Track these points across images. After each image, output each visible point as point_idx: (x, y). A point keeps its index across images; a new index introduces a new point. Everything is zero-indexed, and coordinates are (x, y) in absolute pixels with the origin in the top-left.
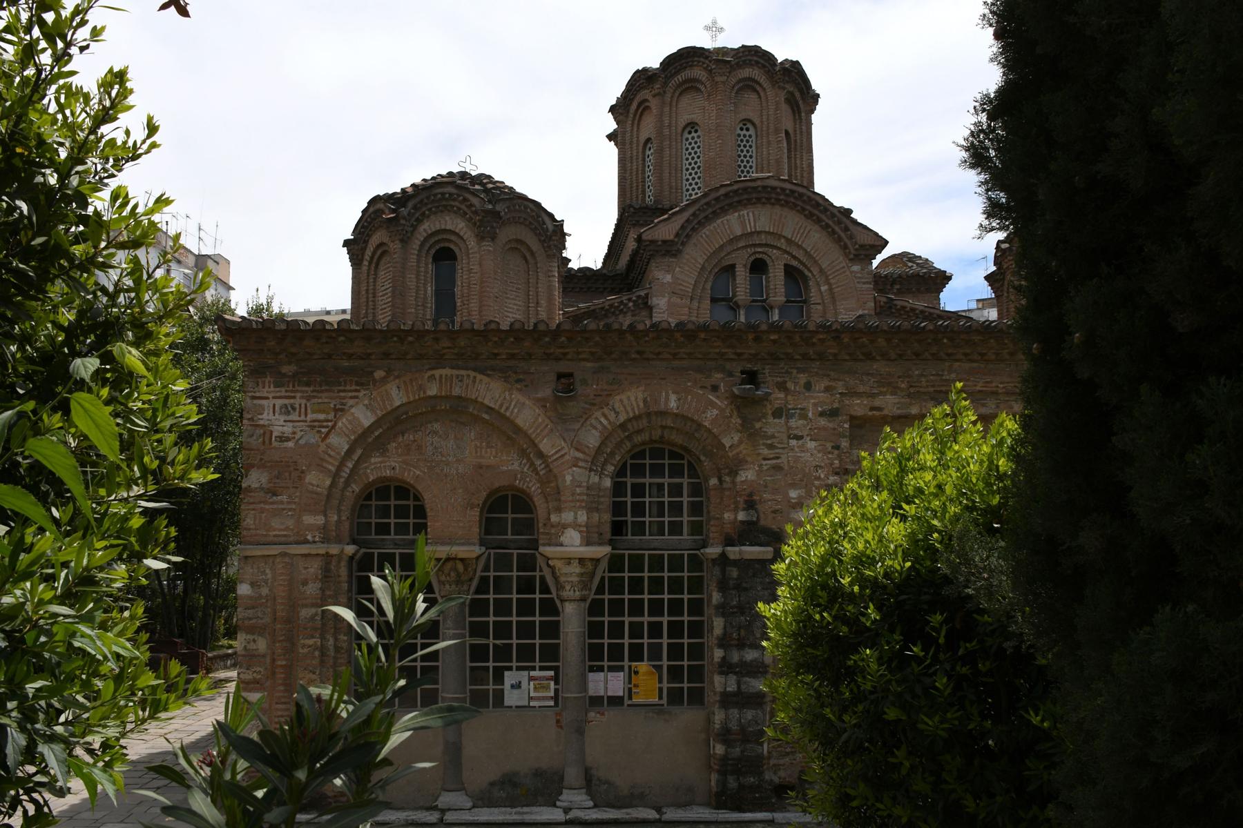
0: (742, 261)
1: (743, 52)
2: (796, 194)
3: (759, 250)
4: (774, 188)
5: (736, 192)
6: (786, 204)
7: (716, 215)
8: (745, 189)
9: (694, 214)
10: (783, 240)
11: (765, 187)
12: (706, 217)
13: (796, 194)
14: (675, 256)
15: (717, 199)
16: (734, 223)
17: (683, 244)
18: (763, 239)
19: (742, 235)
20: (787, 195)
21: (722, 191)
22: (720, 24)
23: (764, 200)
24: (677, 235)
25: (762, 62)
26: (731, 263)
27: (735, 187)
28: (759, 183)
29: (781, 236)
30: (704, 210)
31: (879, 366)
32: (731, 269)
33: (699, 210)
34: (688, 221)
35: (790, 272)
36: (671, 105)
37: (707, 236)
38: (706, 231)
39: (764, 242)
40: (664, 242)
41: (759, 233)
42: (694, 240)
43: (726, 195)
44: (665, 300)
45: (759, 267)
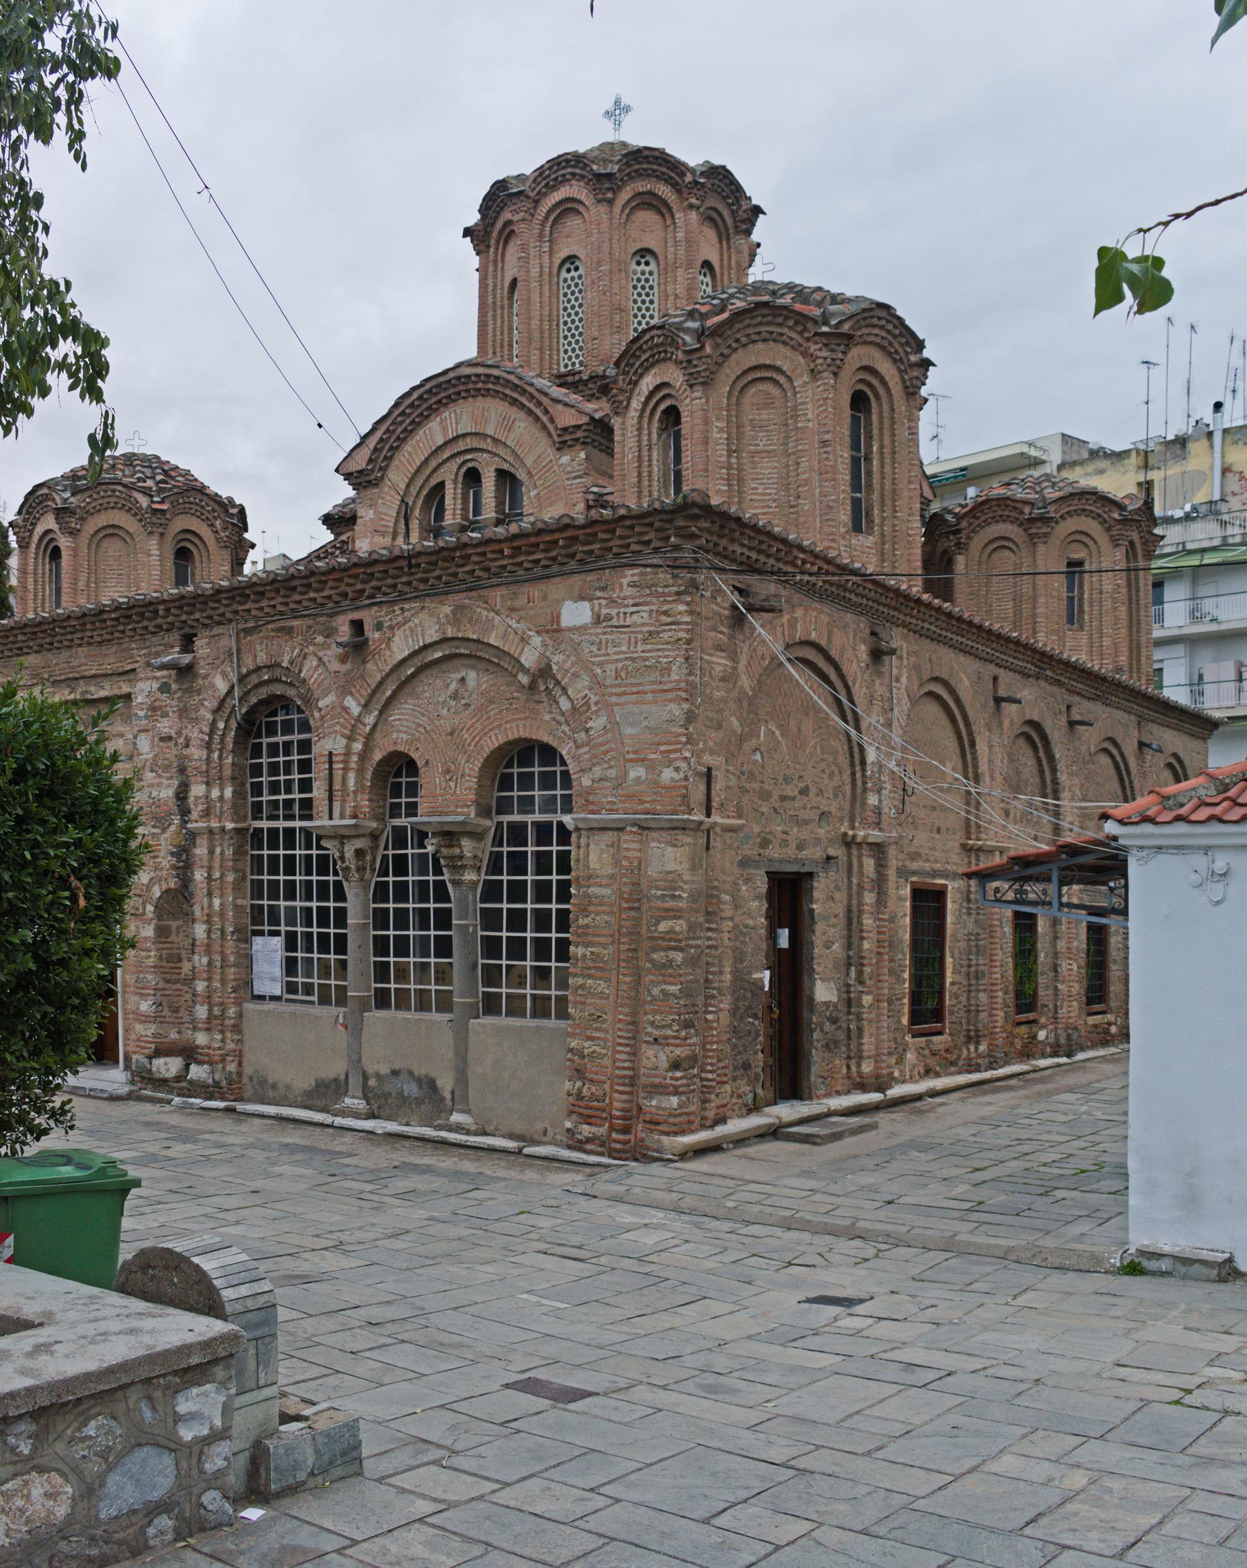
0: (449, 475)
1: (550, 168)
2: (482, 378)
3: (469, 457)
4: (468, 377)
5: (430, 391)
6: (487, 393)
7: (416, 425)
8: (439, 386)
9: (387, 431)
10: (489, 440)
11: (459, 378)
12: (405, 430)
13: (482, 378)
14: (376, 485)
15: (412, 405)
16: (434, 432)
17: (384, 469)
18: (469, 443)
19: (446, 444)
20: (483, 382)
21: (415, 396)
22: (609, 105)
23: (463, 394)
24: (370, 461)
25: (578, 171)
26: (440, 480)
27: (427, 388)
28: (451, 375)
29: (485, 436)
30: (401, 423)
31: (32, 660)
32: (441, 486)
33: (393, 423)
34: (381, 440)
35: (505, 478)
36: (495, 262)
37: (410, 454)
38: (408, 447)
39: (469, 447)
40: (360, 472)
41: (464, 435)
42: (395, 462)
43: (420, 398)
44: (367, 541)
45: (473, 477)
